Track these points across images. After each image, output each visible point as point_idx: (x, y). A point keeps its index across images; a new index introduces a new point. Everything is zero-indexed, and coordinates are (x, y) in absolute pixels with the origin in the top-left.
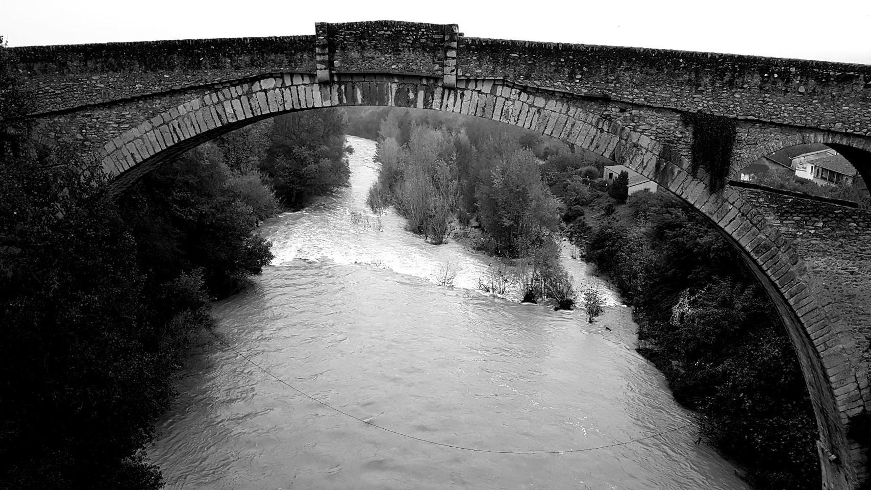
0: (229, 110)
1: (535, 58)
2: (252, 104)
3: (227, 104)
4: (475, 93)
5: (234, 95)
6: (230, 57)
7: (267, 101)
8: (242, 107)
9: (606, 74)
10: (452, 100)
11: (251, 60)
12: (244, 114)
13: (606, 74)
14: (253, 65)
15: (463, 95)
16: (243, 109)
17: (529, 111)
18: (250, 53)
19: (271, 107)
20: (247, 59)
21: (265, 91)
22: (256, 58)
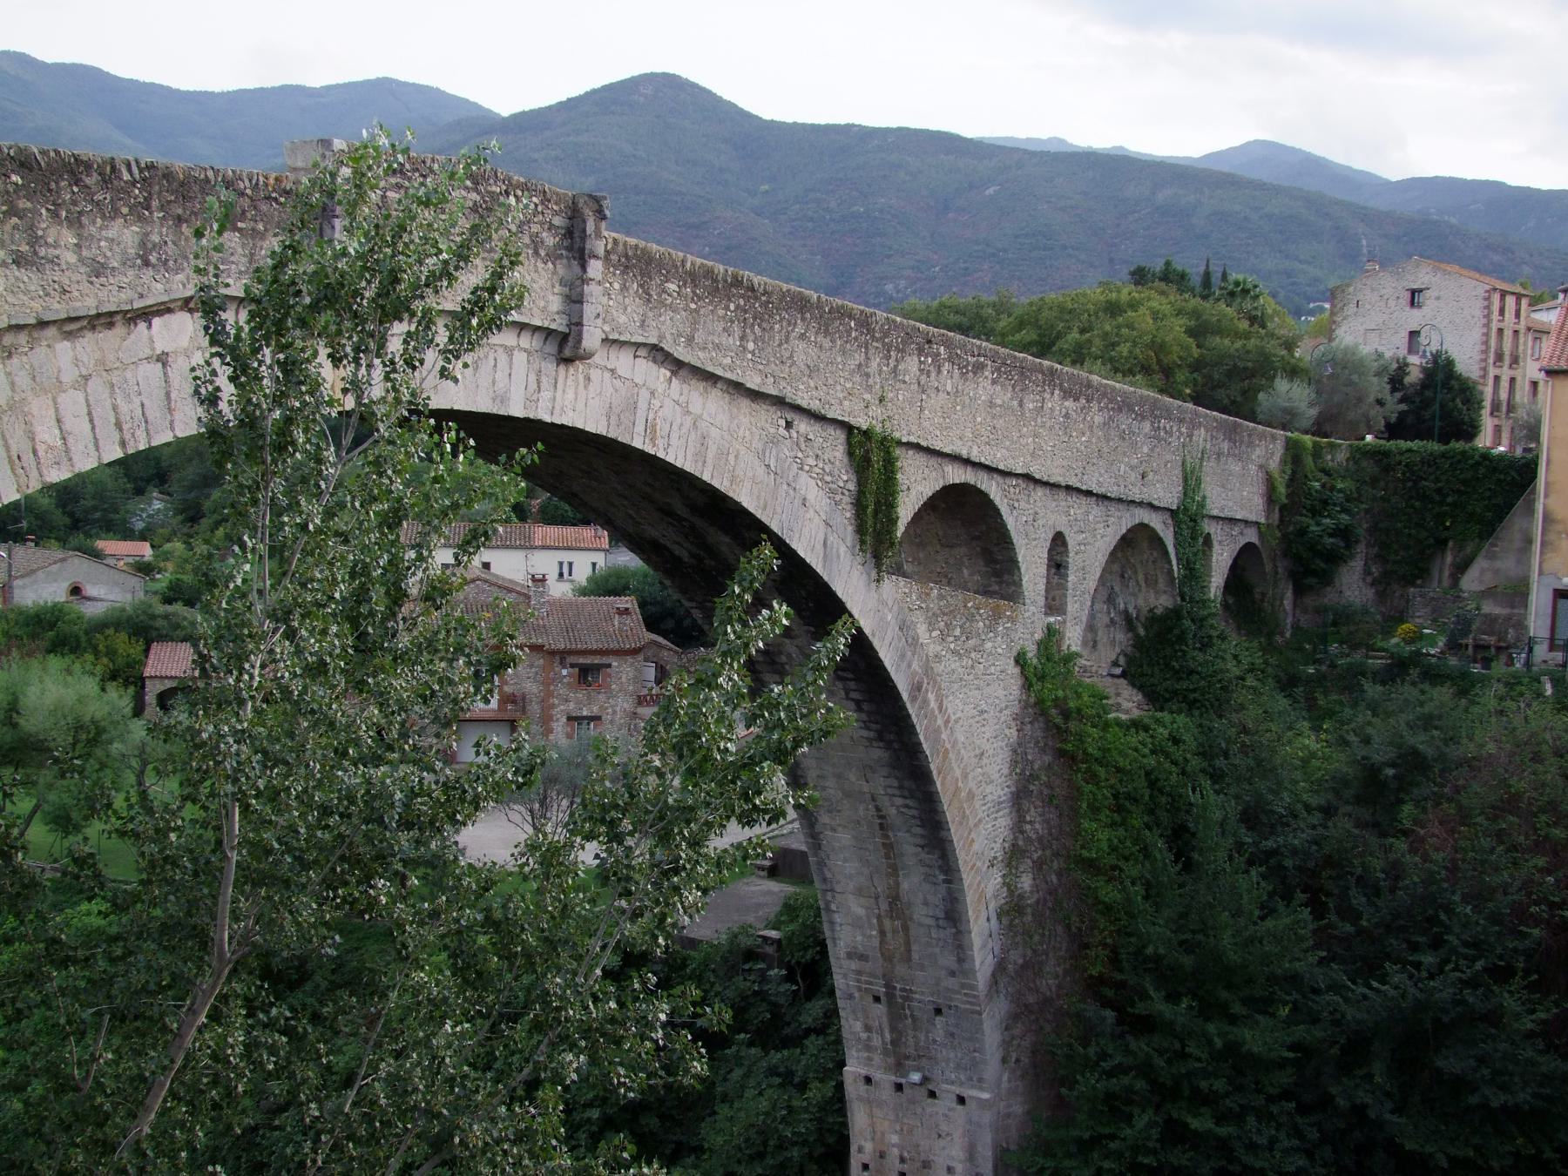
0: (47, 434)
1: (700, 298)
2: (124, 408)
3: (41, 409)
4: (607, 375)
5: (70, 375)
6: (75, 222)
7: (168, 394)
8: (91, 421)
9: (780, 345)
10: (570, 395)
11: (143, 244)
12: (97, 448)
13: (780, 345)
14: (147, 263)
15: (588, 379)
16: (93, 428)
17: (682, 425)
18: (141, 218)
19: (178, 416)
20: (125, 234)
21: (163, 359)
22: (156, 238)
